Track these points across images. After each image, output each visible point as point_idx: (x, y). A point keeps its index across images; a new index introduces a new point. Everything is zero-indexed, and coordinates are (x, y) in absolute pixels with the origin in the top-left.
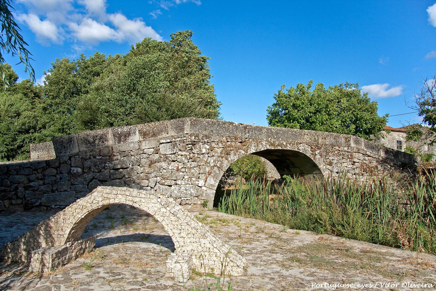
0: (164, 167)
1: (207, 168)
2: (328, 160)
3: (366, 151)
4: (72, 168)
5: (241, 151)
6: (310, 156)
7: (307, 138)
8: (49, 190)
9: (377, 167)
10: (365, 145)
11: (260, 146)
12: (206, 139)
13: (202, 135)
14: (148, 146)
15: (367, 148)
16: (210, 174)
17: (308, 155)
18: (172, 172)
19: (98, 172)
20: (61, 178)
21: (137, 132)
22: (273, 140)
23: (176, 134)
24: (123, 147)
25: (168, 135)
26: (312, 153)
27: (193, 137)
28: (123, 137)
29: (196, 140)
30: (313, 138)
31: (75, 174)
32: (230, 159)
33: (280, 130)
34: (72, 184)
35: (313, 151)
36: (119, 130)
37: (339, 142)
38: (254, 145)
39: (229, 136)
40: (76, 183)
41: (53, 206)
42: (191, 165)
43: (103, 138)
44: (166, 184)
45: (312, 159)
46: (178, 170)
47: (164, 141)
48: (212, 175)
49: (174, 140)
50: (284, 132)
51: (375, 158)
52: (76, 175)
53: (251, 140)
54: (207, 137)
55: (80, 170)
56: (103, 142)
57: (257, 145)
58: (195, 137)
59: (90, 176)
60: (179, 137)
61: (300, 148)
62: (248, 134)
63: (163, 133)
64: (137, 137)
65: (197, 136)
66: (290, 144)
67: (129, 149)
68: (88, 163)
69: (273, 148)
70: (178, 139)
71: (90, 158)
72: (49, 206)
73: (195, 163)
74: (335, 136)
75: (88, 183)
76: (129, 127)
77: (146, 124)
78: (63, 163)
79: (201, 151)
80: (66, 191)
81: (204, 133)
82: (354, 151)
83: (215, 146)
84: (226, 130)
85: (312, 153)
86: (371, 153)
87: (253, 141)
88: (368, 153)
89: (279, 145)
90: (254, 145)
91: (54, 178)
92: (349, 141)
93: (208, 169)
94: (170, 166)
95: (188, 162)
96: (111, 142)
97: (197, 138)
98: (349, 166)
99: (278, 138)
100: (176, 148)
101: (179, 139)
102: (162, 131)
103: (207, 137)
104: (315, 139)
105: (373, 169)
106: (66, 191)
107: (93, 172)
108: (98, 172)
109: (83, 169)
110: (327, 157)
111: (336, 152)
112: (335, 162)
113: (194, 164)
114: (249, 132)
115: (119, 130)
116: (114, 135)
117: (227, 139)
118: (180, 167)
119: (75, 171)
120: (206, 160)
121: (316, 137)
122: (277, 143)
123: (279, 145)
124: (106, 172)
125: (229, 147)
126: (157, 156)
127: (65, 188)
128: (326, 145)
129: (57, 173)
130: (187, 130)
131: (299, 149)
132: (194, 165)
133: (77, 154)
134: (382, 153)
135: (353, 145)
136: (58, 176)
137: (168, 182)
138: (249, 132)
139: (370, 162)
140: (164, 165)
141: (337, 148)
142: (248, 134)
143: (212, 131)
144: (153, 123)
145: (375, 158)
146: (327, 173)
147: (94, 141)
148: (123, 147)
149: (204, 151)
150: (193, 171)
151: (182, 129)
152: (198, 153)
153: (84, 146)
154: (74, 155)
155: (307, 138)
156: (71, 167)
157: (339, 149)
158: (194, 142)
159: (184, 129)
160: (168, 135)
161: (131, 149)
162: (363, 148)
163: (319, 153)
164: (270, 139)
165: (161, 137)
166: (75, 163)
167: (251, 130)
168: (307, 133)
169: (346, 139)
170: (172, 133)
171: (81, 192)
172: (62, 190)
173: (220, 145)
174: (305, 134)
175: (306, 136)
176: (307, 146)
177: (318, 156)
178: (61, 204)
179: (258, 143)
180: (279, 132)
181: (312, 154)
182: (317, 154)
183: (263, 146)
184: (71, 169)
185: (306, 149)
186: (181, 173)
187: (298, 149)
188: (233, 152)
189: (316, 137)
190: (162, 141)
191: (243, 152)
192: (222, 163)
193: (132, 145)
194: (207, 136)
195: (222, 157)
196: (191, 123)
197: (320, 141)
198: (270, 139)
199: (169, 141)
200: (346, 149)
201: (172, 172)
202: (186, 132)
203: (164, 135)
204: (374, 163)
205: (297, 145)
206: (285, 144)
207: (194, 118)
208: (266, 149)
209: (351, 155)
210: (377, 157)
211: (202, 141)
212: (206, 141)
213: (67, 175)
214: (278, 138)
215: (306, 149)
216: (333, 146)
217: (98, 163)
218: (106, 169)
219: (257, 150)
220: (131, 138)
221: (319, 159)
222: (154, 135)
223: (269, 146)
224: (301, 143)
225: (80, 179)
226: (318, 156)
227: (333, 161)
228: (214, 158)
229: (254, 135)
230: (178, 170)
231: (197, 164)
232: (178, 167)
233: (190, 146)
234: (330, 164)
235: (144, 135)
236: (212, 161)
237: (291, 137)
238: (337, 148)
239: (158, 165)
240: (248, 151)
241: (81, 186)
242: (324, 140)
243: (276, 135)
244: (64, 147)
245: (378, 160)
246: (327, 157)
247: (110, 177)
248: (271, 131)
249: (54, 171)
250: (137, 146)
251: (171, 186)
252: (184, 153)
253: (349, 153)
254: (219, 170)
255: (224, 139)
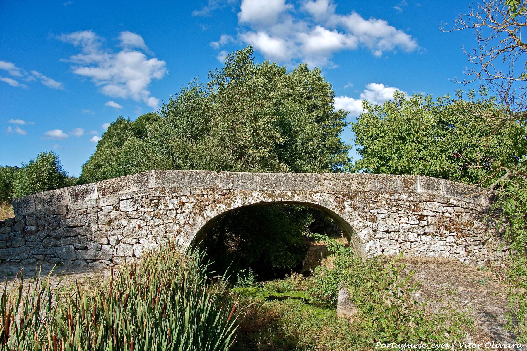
0: (125, 225)
1: (175, 226)
2: (368, 214)
3: (448, 199)
4: (27, 227)
5: (220, 205)
6: (334, 209)
7: (328, 185)
8: (3, 245)
9: (472, 224)
10: (447, 189)
11: (251, 198)
12: (174, 193)
13: (169, 189)
14: (106, 204)
15: (452, 194)
16: (178, 233)
17: (330, 207)
18: (133, 230)
19: (53, 230)
20: (15, 236)
21: (96, 189)
22: (270, 190)
23: (139, 189)
24: (81, 205)
25: (129, 191)
26: (337, 204)
27: (158, 192)
28: (80, 195)
29: (161, 195)
30: (341, 184)
31: (29, 231)
32: (205, 216)
33: (282, 177)
34: (26, 241)
35: (340, 202)
36: (76, 188)
37: (392, 187)
38: (240, 197)
39: (204, 189)
40: (30, 240)
41: (8, 260)
42: (155, 222)
43: (60, 198)
44: (127, 242)
45: (337, 213)
46: (140, 228)
47: (125, 198)
48: (183, 234)
49: (135, 196)
50: (289, 179)
51: (468, 208)
52: (31, 233)
53: (236, 192)
54: (175, 190)
55: (34, 228)
56: (60, 201)
57: (245, 197)
58: (160, 191)
59: (44, 233)
60: (141, 193)
61: (315, 199)
62: (232, 185)
63: (124, 189)
64: (95, 195)
65: (163, 190)
66: (298, 194)
67: (84, 207)
68: (42, 222)
69: (270, 201)
70: (139, 195)
71: (45, 217)
72: (4, 260)
73: (160, 221)
74: (384, 179)
75: (43, 240)
76: (88, 185)
77: (105, 181)
78: (18, 222)
79: (168, 207)
80: (20, 247)
81: (172, 186)
82: (423, 198)
83: (186, 201)
84: (201, 181)
85: (337, 204)
86: (459, 201)
87: (240, 193)
88: (452, 201)
89: (279, 196)
90: (240, 197)
91: (8, 236)
92: (412, 184)
93: (175, 227)
94: (131, 224)
95: (152, 219)
96: (68, 200)
97: (163, 192)
98: (412, 222)
99: (278, 188)
100: (136, 204)
101: (141, 194)
102: (123, 187)
103: (175, 190)
104: (344, 184)
105: (463, 227)
106: (20, 247)
107: (47, 229)
108: (53, 230)
109: (38, 226)
110: (366, 210)
111: (384, 202)
112: (383, 216)
113: (158, 222)
114: (233, 182)
115: (76, 188)
116: (71, 194)
117: (201, 192)
118: (142, 225)
119: (29, 229)
120: (174, 217)
121: (346, 182)
122: (277, 193)
123: (279, 196)
124: (60, 230)
125: (205, 200)
126: (115, 214)
127: (19, 244)
128: (366, 192)
129: (11, 231)
130: (152, 184)
131: (315, 201)
132: (158, 223)
133: (33, 214)
134: (483, 201)
135: (419, 189)
136: (12, 234)
137: (129, 241)
138: (233, 182)
139: (458, 216)
140: (124, 222)
141: (387, 196)
142: (232, 185)
143: (182, 184)
144: (113, 179)
145: (468, 208)
146: (367, 232)
147: (51, 201)
148: (81, 205)
149: (171, 207)
150: (157, 229)
151: (146, 184)
152: (164, 209)
153: (41, 205)
154: (29, 215)
155: (328, 185)
156: (26, 225)
157: (391, 198)
158: (160, 197)
159: (148, 183)
160: (129, 191)
161: (88, 207)
162: (442, 193)
163: (350, 205)
164: (265, 188)
165: (121, 193)
166: (29, 221)
167: (237, 179)
168: (330, 177)
169: (406, 181)
170: (134, 188)
171: (34, 248)
172: (16, 246)
173: (192, 199)
174: (325, 179)
175: (327, 182)
176: (328, 195)
177: (349, 209)
178: (16, 258)
179: (246, 193)
180: (280, 178)
181: (338, 207)
182: (346, 205)
183: (253, 199)
184: (24, 227)
185: (326, 200)
186: (144, 232)
187: (312, 200)
188: (210, 206)
189: (346, 182)
190: (121, 198)
191: (224, 207)
192: (195, 219)
193: (89, 203)
194: (175, 189)
195: (196, 214)
196: (157, 176)
197: (354, 187)
198: (265, 188)
199: (129, 197)
200: (405, 197)
201: (133, 230)
202: (150, 187)
203: (125, 191)
204: (467, 217)
205: (310, 194)
206: (290, 194)
207: (161, 170)
208: (258, 201)
209: (415, 206)
210: (472, 206)
211: (168, 195)
212: (174, 195)
213: (20, 232)
214: (278, 188)
215: (326, 200)
216: (378, 193)
217: (52, 221)
218: (60, 227)
219: (244, 203)
220: (88, 196)
221: (350, 213)
222: (114, 191)
223: (264, 197)
224: (317, 192)
225: (33, 236)
226: (349, 209)
227: (378, 216)
228: (185, 214)
229: (241, 185)
230: (140, 228)
231: (162, 221)
232: (139, 225)
233: (155, 201)
234: (373, 219)
235: (104, 192)
236: (182, 218)
237: (300, 184)
238: (387, 196)
239: (117, 222)
240: (232, 205)
241: (35, 242)
242: (361, 186)
243: (276, 183)
244: (22, 207)
245: (474, 212)
246: (366, 210)
247: (64, 234)
248: (268, 179)
249: (9, 229)
250: (94, 204)
251: (133, 245)
252: (146, 210)
253: (412, 203)
254: (192, 229)
255: (198, 191)
